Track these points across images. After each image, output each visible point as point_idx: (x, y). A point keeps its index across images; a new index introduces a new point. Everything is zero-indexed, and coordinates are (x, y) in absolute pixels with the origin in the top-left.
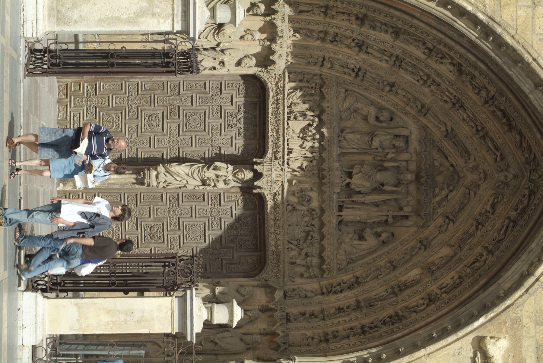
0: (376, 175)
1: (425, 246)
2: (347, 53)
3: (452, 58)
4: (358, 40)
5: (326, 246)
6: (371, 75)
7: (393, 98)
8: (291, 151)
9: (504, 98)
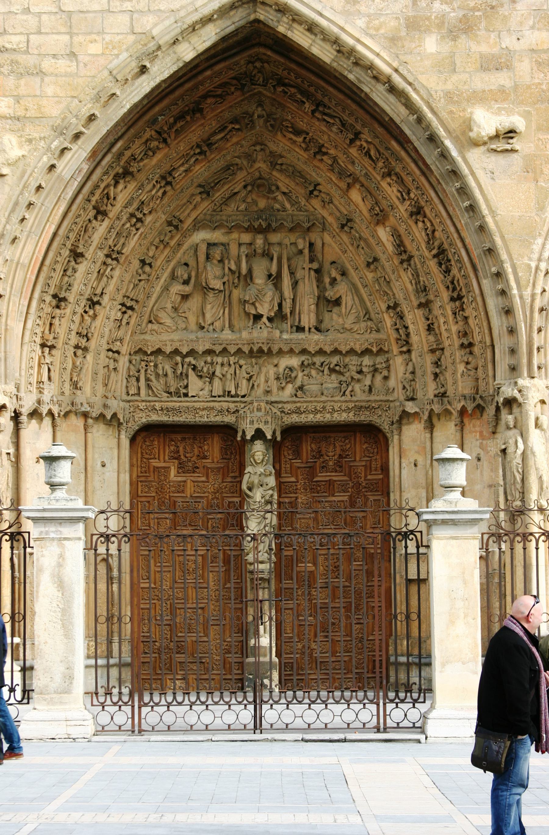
0: (257, 284)
1: (349, 220)
2: (102, 321)
3: (108, 186)
4: (85, 306)
6: (130, 290)
7: (159, 262)
9: (160, 118)
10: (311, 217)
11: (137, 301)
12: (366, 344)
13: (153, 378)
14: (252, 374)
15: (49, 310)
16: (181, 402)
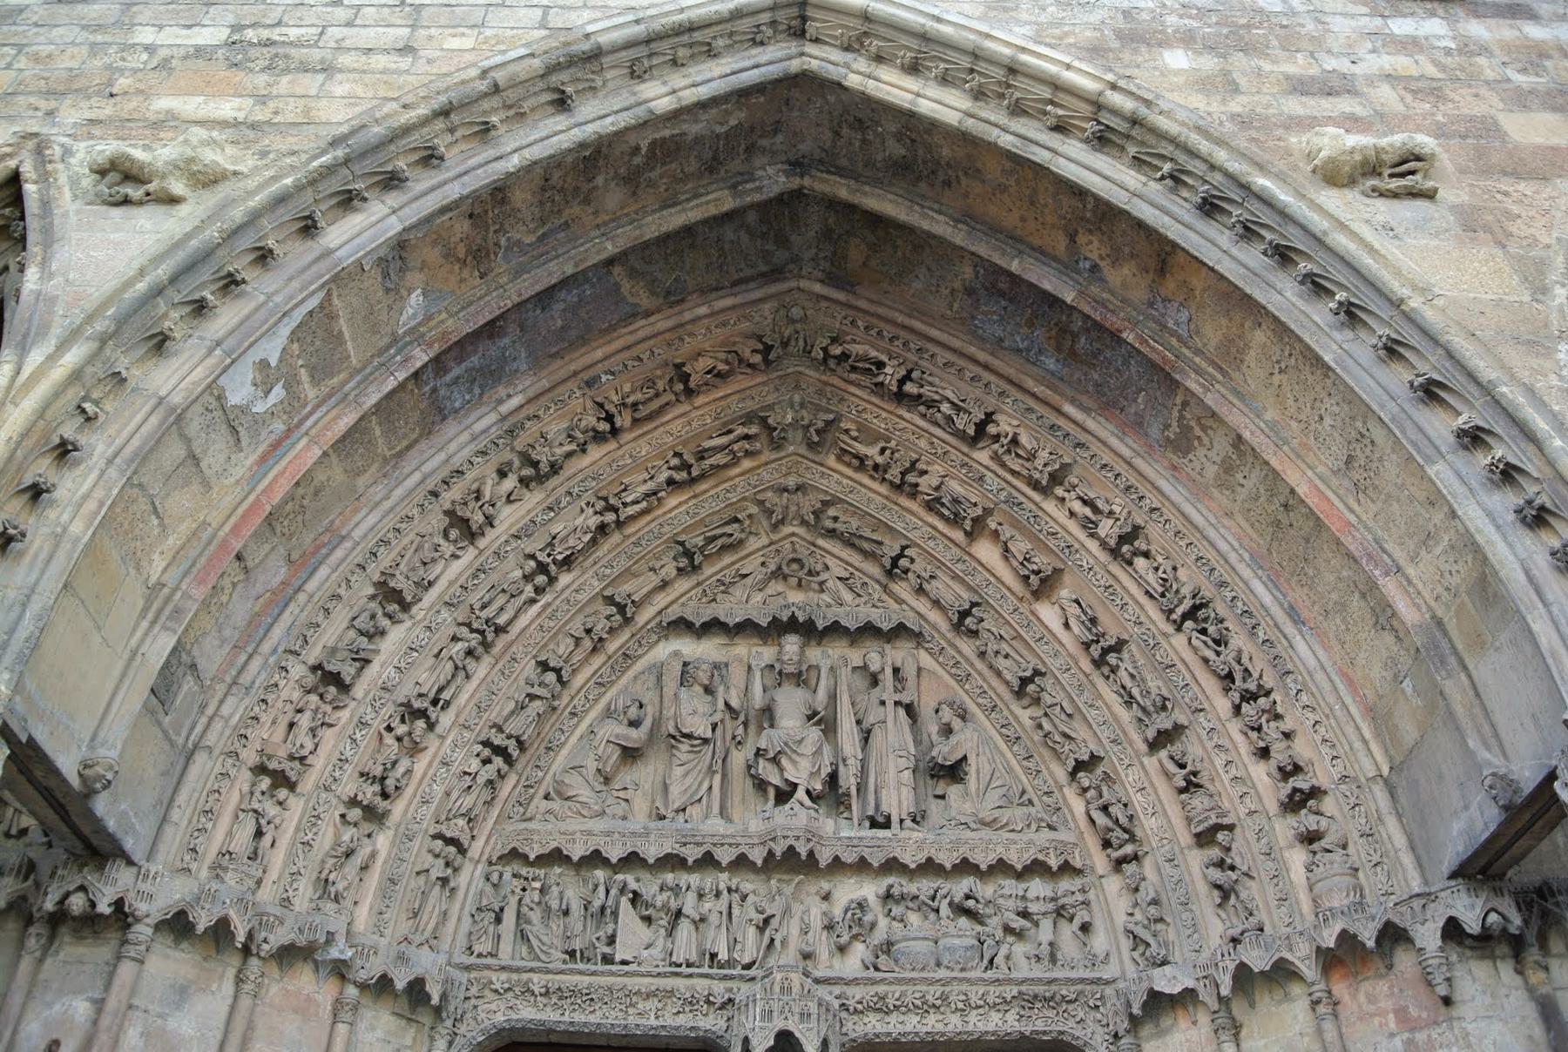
2: (430, 764)
5: (992, 858)
6: (505, 713)
10: (894, 617)
12: (1032, 851)
13: (535, 916)
14: (769, 912)
15: (296, 695)
16: (594, 973)
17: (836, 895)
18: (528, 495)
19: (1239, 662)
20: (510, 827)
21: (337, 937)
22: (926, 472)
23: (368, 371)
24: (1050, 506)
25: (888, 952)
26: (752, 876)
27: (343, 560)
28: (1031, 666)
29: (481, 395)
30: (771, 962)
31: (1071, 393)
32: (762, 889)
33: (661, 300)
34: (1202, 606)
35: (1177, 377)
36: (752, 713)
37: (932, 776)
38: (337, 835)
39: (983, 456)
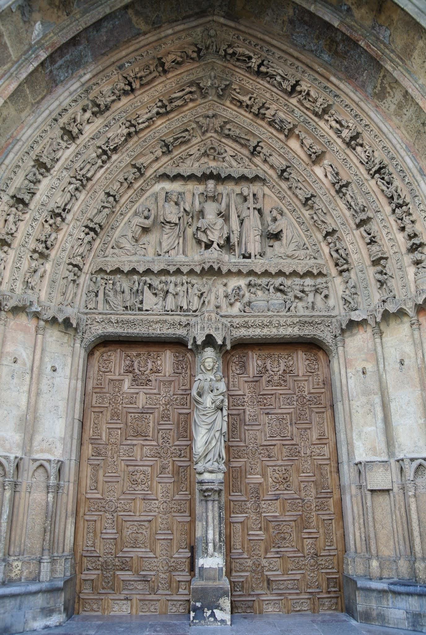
2: (64, 235)
4: (46, 216)
5: (291, 270)
6: (93, 214)
8: (179, 308)
11: (101, 226)
12: (307, 267)
13: (111, 294)
14: (203, 291)
15: (6, 208)
16: (135, 315)
17: (229, 284)
18: (96, 120)
19: (396, 192)
20: (99, 260)
21: (34, 303)
22: (269, 108)
23: (20, 62)
24: (322, 123)
25: (249, 306)
26: (195, 277)
27: (19, 150)
28: (310, 193)
29: (72, 74)
30: (204, 309)
31: (334, 71)
32: (200, 282)
33: (151, 27)
34: (383, 168)
35: (382, 63)
36: (195, 213)
37: (268, 238)
38: (30, 264)
39: (294, 101)
